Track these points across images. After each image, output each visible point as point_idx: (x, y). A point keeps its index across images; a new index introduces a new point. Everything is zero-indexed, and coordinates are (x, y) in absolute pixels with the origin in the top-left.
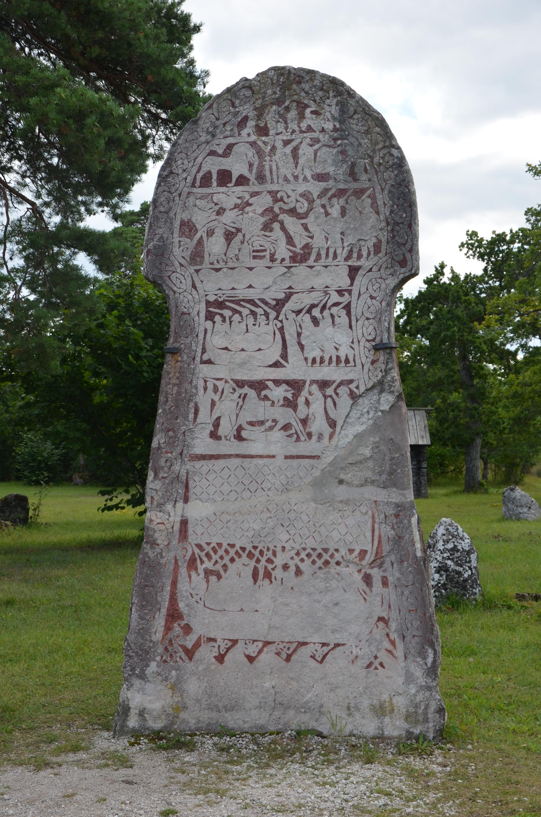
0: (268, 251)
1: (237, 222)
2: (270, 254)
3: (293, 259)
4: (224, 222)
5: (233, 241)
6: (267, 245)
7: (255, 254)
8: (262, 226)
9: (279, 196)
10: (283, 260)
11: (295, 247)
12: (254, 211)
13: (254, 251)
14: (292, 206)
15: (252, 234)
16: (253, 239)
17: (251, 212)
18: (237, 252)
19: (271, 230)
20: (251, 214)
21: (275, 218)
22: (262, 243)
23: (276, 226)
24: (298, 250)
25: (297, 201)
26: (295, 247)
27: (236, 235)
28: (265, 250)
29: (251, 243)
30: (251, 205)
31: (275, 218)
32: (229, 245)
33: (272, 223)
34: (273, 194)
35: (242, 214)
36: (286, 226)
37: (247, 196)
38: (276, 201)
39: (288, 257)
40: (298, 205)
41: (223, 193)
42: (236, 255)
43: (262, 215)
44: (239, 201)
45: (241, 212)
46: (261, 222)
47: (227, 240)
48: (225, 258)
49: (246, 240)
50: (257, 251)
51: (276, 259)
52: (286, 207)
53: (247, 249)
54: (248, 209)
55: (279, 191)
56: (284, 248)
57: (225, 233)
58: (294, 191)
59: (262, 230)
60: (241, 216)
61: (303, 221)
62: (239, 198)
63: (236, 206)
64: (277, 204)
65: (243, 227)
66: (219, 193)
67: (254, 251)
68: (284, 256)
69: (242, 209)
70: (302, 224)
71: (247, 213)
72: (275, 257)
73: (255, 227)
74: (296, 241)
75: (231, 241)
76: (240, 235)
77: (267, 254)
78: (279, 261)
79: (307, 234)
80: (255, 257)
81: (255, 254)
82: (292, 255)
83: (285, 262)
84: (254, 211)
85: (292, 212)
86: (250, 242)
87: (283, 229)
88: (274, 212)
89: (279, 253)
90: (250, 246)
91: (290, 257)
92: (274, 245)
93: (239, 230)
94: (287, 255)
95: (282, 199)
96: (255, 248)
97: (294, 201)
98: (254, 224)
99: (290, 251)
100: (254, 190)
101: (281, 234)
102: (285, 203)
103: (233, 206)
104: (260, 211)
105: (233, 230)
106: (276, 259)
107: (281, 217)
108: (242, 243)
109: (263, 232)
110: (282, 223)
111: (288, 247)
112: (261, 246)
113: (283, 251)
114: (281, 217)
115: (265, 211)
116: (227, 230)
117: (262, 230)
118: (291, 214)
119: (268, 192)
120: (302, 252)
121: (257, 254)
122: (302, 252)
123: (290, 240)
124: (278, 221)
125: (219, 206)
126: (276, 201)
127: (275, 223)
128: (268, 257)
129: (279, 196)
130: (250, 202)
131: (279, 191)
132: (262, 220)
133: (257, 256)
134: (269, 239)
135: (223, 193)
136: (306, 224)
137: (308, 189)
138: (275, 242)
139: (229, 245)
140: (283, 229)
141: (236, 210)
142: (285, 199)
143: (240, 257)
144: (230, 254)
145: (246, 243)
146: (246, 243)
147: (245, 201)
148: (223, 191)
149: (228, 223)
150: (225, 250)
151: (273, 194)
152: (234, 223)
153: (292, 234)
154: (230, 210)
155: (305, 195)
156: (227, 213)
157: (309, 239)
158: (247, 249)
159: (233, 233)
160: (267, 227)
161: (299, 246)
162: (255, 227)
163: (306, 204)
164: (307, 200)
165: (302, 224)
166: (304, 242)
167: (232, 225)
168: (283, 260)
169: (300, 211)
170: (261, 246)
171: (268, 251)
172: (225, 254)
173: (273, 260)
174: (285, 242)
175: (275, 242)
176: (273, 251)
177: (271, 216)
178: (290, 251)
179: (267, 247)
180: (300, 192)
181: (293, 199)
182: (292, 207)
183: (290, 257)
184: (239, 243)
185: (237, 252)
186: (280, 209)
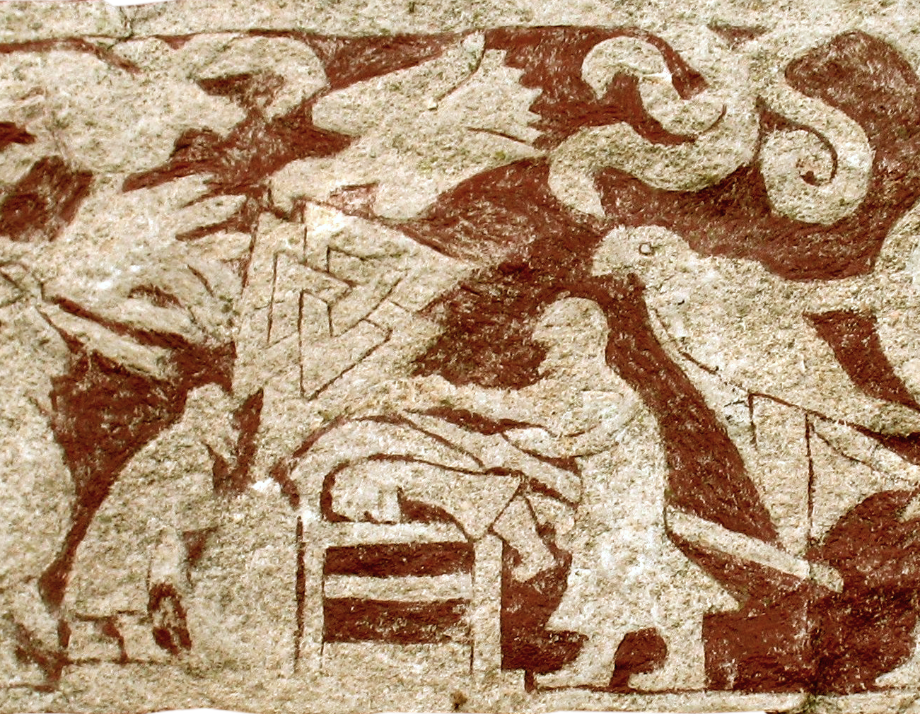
0: (488, 560)
1: (188, 289)
2: (510, 590)
3: (747, 645)
4: (65, 285)
5: (138, 463)
6: (476, 509)
7: (351, 586)
8: (429, 331)
9: (596, 70)
10: (641, 651)
11: (763, 528)
12: (360, 201)
13: (342, 561)
14: (723, 155)
15: (333, 401)
16: (334, 447)
17: (336, 200)
18: (168, 568)
19: (522, 368)
20: (324, 224)
21: (556, 261)
22: (426, 485)
23: (569, 329)
24: (787, 560)
25: (771, 121)
26: (763, 528)
27: (176, 406)
28: (457, 556)
29: (311, 485)
30: (331, 144)
31: (556, 261)
32: (90, 496)
33: (530, 307)
34: (549, 57)
35: (243, 222)
36: (670, 328)
37: (300, 75)
38: (568, 110)
39: (693, 625)
40: (780, 158)
41: (77, 43)
42: (160, 594)
43: (436, 226)
44: (222, 115)
45: (230, 204)
46: (425, 293)
47: (74, 446)
48: (42, 623)
49: (266, 455)
50: (377, 561)
51: (571, 645)
52: (662, 172)
53: (268, 539)
54: (289, 181)
55: (595, 36)
56: (651, 539)
57: (62, 388)
58: (735, 35)
59: (423, 364)
60: (233, 242)
61: (834, 295)
62: (220, 86)
63: (191, 153)
64: (572, 144)
65: (246, 332)
66: (41, 46)
67: (342, 561)
68: (651, 617)
69: (248, 181)
70: (825, 324)
71: (295, 213)
72: (557, 622)
73: (362, 339)
74: (774, 472)
75: (118, 458)
76: (209, 413)
77: (479, 592)
78: (596, 660)
79: (868, 408)
80: (346, 622)
81: (351, 586)
82: (726, 602)
83: (664, 676)
84: (360, 201)
85: (729, 207)
86: (308, 476)
87: (637, 350)
88: (552, 206)
89: (605, 586)
90: (309, 514)
91: (713, 623)
92: (549, 508)
93: (201, 362)
94: (683, 606)
95: (624, 102)
96: (358, 534)
97: (742, 113)
98: (353, 307)
99: (716, 566)
100: (363, 27)
101: (615, 402)
102: (653, 131)
103: (162, 155)
104: (417, 192)
105: (149, 360)
106: (571, 645)
107: (618, 251)
108: (229, 478)
109: (440, 387)
110: (625, 308)
111: (691, 526)
112: (415, 512)
113: (633, 562)
114: (618, 251)
115: (463, 195)
116: (83, 361)
117: (423, 364)
118: (717, 230)
119: (498, 38)
120: (831, 580)
121: (374, 596)
122: (831, 580)
123: (705, 466)
124: (597, 291)
125: (35, 152)
126: (568, 110)
127: (561, 309)
128: (485, 618)
129: (596, 70)
130: (326, 116)
131: (595, 36)
132: (434, 272)
133: (367, 608)
134: (496, 451)
135: (77, 43)
136: (865, 323)
137: (872, 25)
138: (558, 479)
139: (90, 496)
140: (637, 350)
141: (191, 185)
142: (663, 106)
143: (202, 615)
144: (110, 582)
145: (264, 485)
146: (264, 485)
147: (278, 108)
148: (85, 28)
149: (97, 293)
150: (50, 550)
151: (549, 57)
152: (161, 297)
153: (719, 399)
154: (136, 182)
155: (838, 72)
156: (106, 209)
157: (889, 458)
158: (268, 539)
159: (140, 384)
160: (480, 338)
161: (794, 531)
162: (362, 339)
163: (856, 151)
164: (863, 118)
165: (825, 324)
166: (845, 488)
167: (140, 311)
168: (641, 651)
169: (790, 200)
170: (415, 512)
171: (488, 560)
172: (53, 586)
173: (533, 646)
174: (656, 479)
175: (558, 479)
176: (536, 560)
177: (519, 241)
178: (716, 566)
179: (472, 519)
180: (790, 53)
181: (730, 94)
182: (724, 165)
183: (713, 623)
184: (199, 484)
185: (168, 568)
186: (611, 181)
